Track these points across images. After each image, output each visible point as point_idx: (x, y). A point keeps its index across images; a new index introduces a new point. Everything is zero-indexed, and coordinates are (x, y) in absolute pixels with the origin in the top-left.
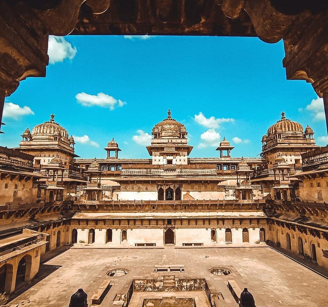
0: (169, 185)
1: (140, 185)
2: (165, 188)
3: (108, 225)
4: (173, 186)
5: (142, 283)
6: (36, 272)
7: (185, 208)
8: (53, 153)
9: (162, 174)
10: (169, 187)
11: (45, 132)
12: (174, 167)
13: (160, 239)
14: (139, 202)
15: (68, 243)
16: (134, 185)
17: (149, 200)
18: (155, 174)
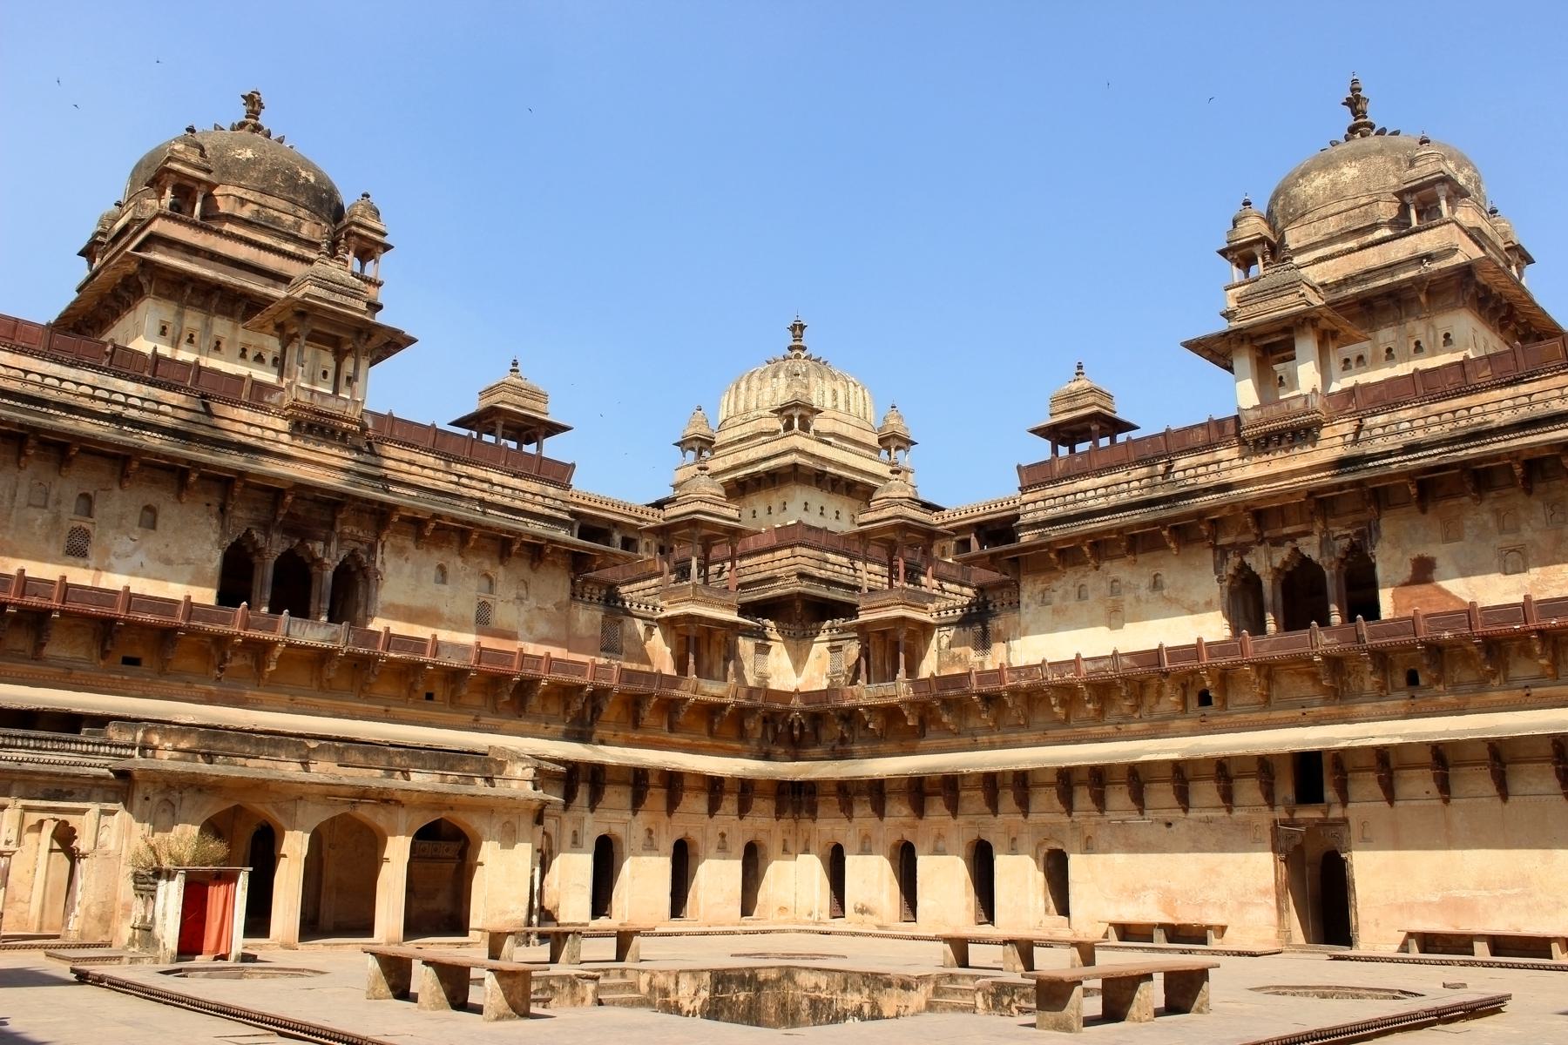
0: (1292, 537)
1: (1119, 570)
2: (1265, 563)
3: (971, 818)
4: (1315, 539)
5: (824, 986)
6: (507, 917)
7: (1412, 679)
8: (780, 494)
9: (1237, 475)
10: (1296, 550)
13: (1257, 904)
14: (1101, 664)
16: (1084, 576)
17: (1156, 647)
18: (1202, 480)
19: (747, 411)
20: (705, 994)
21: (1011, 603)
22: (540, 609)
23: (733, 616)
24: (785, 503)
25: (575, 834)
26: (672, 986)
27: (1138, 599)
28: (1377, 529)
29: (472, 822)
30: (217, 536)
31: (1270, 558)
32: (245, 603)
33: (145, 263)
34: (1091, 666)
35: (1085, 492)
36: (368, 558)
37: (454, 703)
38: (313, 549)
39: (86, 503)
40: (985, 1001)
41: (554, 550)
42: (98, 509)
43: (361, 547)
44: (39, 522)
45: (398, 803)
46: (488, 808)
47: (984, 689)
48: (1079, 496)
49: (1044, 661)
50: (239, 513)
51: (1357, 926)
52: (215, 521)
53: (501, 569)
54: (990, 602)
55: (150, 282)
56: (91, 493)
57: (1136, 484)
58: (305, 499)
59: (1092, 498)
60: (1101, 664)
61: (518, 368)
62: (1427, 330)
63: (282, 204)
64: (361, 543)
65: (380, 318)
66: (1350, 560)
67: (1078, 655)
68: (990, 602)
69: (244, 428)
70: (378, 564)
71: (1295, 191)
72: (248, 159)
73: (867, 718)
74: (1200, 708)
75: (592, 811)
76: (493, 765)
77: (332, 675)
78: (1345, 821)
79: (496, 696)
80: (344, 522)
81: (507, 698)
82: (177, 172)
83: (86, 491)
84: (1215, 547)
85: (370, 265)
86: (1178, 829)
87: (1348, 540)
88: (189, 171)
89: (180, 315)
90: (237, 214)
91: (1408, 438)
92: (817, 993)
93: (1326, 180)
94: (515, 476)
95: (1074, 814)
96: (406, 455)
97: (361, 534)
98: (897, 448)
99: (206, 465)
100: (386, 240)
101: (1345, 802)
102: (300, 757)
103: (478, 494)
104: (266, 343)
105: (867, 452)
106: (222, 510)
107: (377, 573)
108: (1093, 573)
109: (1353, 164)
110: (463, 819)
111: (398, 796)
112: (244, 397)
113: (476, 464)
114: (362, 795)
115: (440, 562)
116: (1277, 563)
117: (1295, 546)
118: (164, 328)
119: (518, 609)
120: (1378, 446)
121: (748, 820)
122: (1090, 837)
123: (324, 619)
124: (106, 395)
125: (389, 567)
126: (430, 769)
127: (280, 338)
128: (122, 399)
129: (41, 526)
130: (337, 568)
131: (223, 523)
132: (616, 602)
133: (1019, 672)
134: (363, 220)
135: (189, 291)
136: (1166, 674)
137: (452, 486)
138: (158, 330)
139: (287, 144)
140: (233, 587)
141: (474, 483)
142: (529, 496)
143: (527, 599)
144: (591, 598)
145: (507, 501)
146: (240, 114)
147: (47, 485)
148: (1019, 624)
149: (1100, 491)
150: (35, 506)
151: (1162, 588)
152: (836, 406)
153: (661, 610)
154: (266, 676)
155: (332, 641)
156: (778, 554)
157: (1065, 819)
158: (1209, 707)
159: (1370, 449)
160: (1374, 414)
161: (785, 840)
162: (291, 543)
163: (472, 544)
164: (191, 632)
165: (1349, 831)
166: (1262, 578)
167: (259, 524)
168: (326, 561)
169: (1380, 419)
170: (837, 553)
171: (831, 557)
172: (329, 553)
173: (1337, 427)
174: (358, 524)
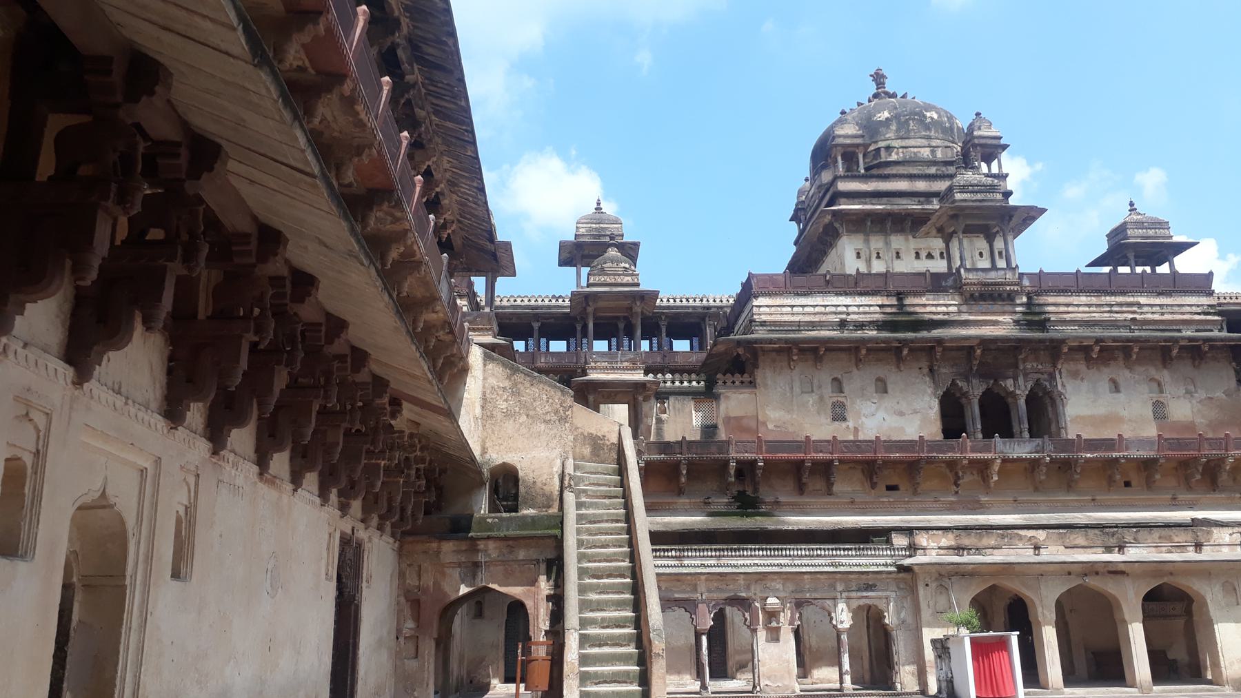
22: (1211, 398)
29: (1197, 586)
30: (931, 389)
32: (964, 434)
33: (835, 213)
37: (1149, 484)
38: (1006, 385)
39: (838, 385)
41: (1211, 347)
42: (846, 388)
44: (811, 402)
45: (1122, 573)
46: (1209, 570)
50: (943, 371)
52: (928, 379)
53: (1165, 373)
55: (842, 225)
56: (839, 376)
58: (991, 350)
61: (1135, 207)
64: (1042, 373)
65: (1013, 201)
69: (933, 309)
70: (1060, 388)
72: (887, 119)
77: (1043, 478)
79: (1187, 479)
80: (1024, 361)
81: (1198, 477)
82: (843, 146)
83: (836, 376)
85: (995, 165)
89: (867, 241)
94: (1160, 294)
96: (1061, 300)
97: (1040, 367)
99: (912, 341)
100: (1003, 142)
104: (931, 244)
106: (931, 370)
107: (1060, 394)
110: (1182, 582)
111: (1122, 567)
113: (1124, 293)
114: (1092, 569)
118: (858, 253)
119: (1190, 402)
123: (1026, 434)
124: (833, 309)
125: (1069, 387)
127: (942, 238)
128: (844, 309)
129: (813, 405)
131: (934, 380)
135: (869, 223)
138: (854, 256)
139: (909, 98)
140: (953, 424)
142: (1176, 309)
143: (1196, 392)
146: (873, 89)
147: (811, 377)
150: (806, 393)
154: (992, 485)
162: (987, 383)
163: (1134, 357)
164: (930, 461)
167: (960, 375)
168: (1018, 392)
172: (1019, 386)
174: (1037, 359)
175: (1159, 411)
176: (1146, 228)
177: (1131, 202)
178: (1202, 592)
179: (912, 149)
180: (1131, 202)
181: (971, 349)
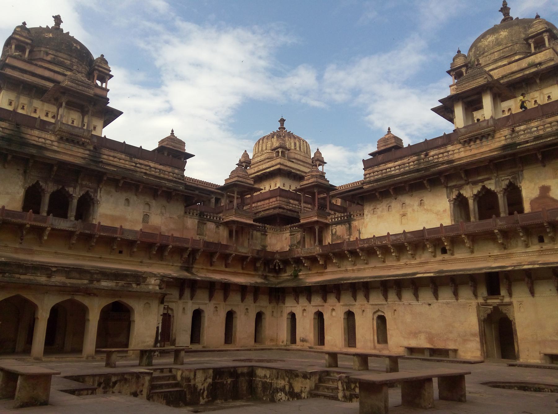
0: (482, 181)
2: (469, 192)
5: (268, 376)
6: (145, 344)
10: (484, 187)
11: (264, 148)
12: (488, 127)
13: (471, 341)
15: (283, 342)
16: (391, 202)
17: (422, 229)
18: (441, 160)
19: (262, 150)
20: (210, 380)
21: (360, 215)
22: (171, 218)
23: (252, 222)
24: (276, 184)
25: (184, 308)
26: (192, 376)
27: (413, 210)
28: (522, 175)
31: (472, 191)
34: (394, 238)
35: (390, 168)
36: (94, 195)
40: (343, 386)
43: (91, 190)
47: (350, 249)
48: (388, 170)
49: (374, 236)
51: (518, 351)
52: (21, 177)
53: (154, 202)
54: (352, 215)
57: (412, 163)
59: (393, 170)
60: (398, 237)
62: (540, 95)
63: (65, 56)
64: (91, 188)
66: (509, 189)
67: (388, 233)
68: (352, 215)
69: (37, 139)
70: (98, 197)
71: (480, 44)
72: (50, 37)
73: (304, 261)
74: (442, 255)
75: (192, 299)
76: (141, 278)
78: (510, 304)
84: (447, 187)
86: (434, 307)
87: (508, 181)
88: (22, 39)
89: (18, 98)
90: (45, 58)
91: (536, 134)
92: (265, 380)
93: (493, 38)
95: (388, 300)
96: (112, 154)
97: (90, 185)
98: (319, 165)
100: (111, 73)
101: (510, 295)
102: (47, 274)
103: (144, 171)
105: (308, 166)
106: (25, 172)
107: (97, 201)
108: (394, 201)
109: (505, 30)
112: (37, 125)
115: (127, 198)
116: (475, 192)
117: (483, 185)
120: (522, 138)
121: (257, 304)
122: (395, 310)
123: (73, 218)
126: (111, 280)
130: (79, 198)
132: (204, 216)
133: (364, 241)
134: (100, 65)
136: (427, 240)
137: (133, 167)
141: (143, 166)
142: (167, 173)
144: (193, 214)
145: (157, 174)
148: (364, 223)
149: (396, 168)
151: (424, 205)
152: (296, 149)
153: (223, 220)
154: (43, 242)
155: (73, 228)
156: (271, 200)
157: (384, 302)
158: (446, 254)
159: (517, 140)
160: (520, 126)
161: (273, 312)
163: (140, 190)
165: (513, 308)
166: (469, 199)
169: (522, 127)
170: (294, 199)
171: (291, 201)
173: (502, 132)
175: (146, 218)
176: (176, 143)
177: (172, 130)
178: (133, 307)
179: (60, 59)
180: (172, 130)
181: (52, 166)
